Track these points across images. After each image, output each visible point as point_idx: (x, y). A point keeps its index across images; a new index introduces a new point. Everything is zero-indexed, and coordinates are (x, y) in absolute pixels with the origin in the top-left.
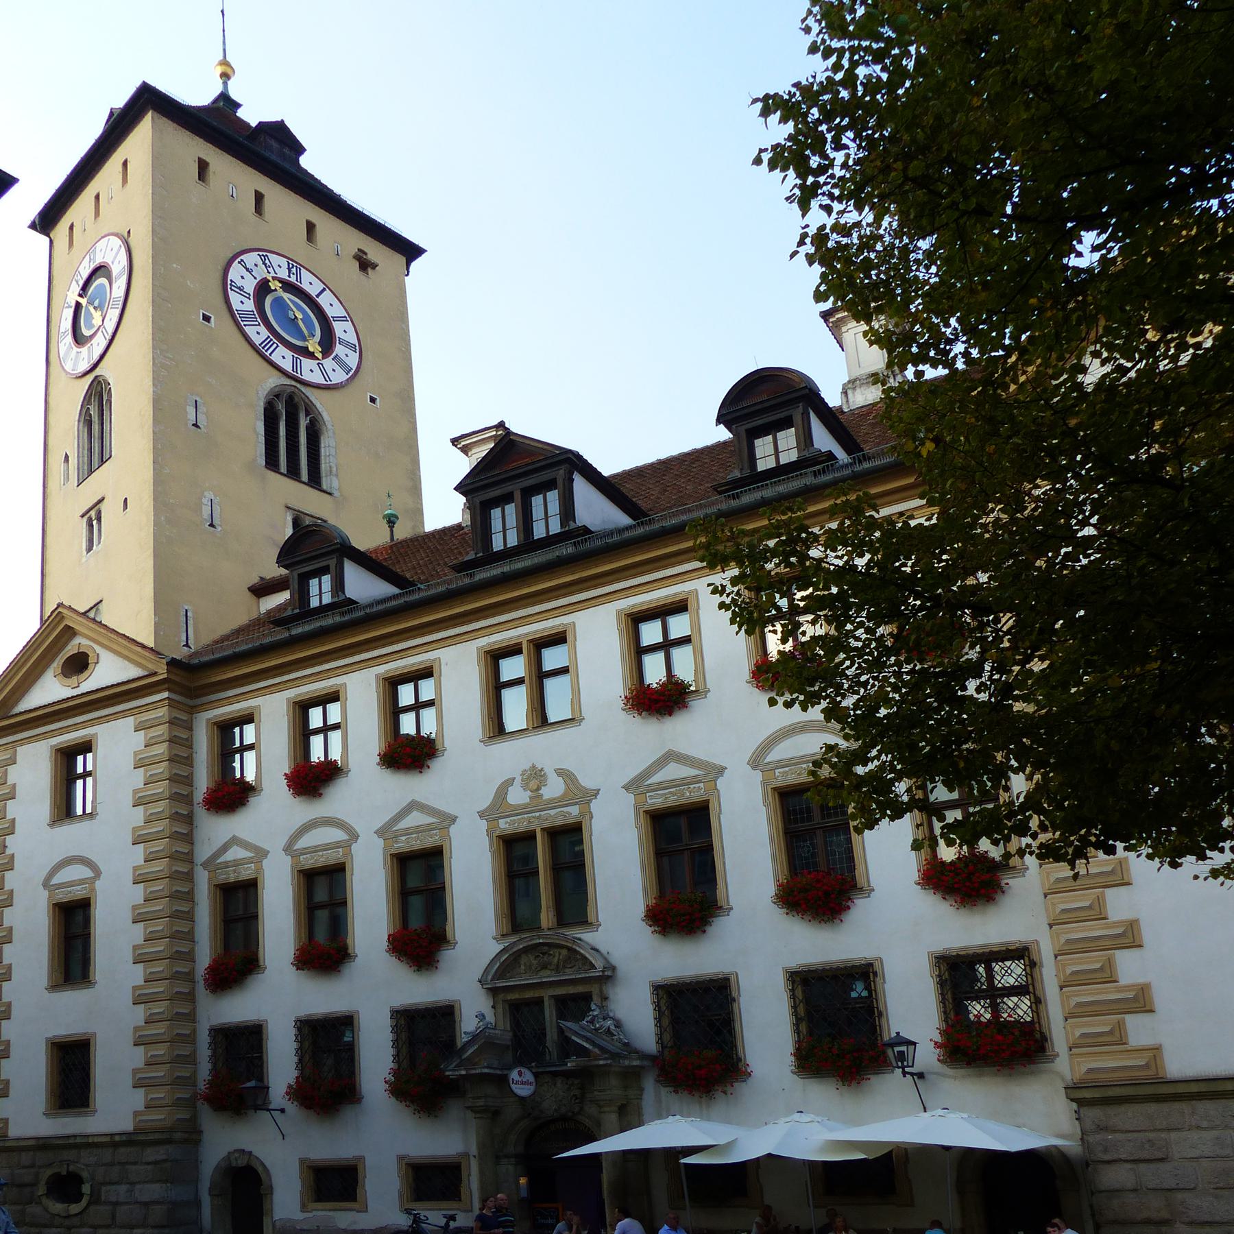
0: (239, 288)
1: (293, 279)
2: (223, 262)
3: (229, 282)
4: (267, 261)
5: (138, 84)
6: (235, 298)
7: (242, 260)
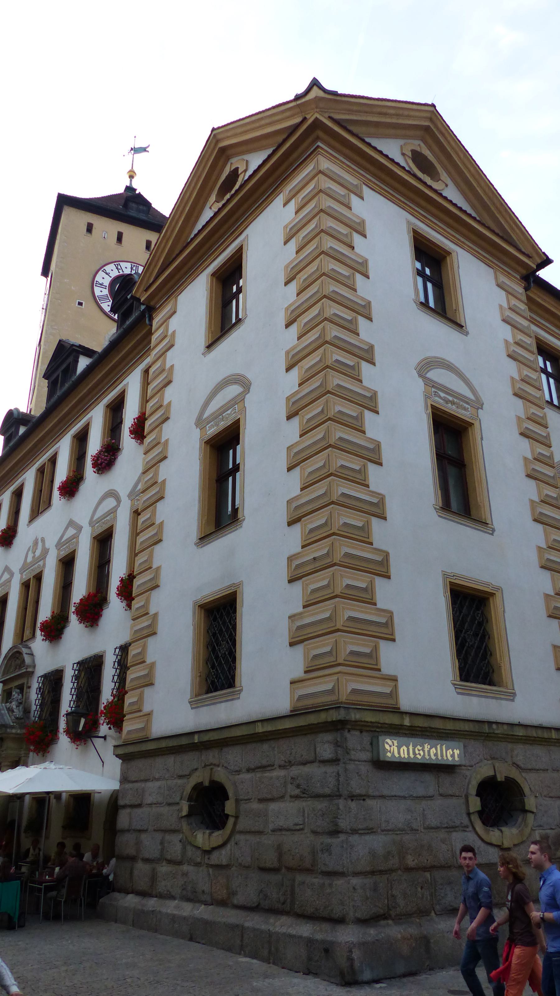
0: (101, 284)
2: (94, 273)
3: (95, 282)
4: (119, 267)
5: (57, 195)
6: (98, 291)
7: (104, 269)
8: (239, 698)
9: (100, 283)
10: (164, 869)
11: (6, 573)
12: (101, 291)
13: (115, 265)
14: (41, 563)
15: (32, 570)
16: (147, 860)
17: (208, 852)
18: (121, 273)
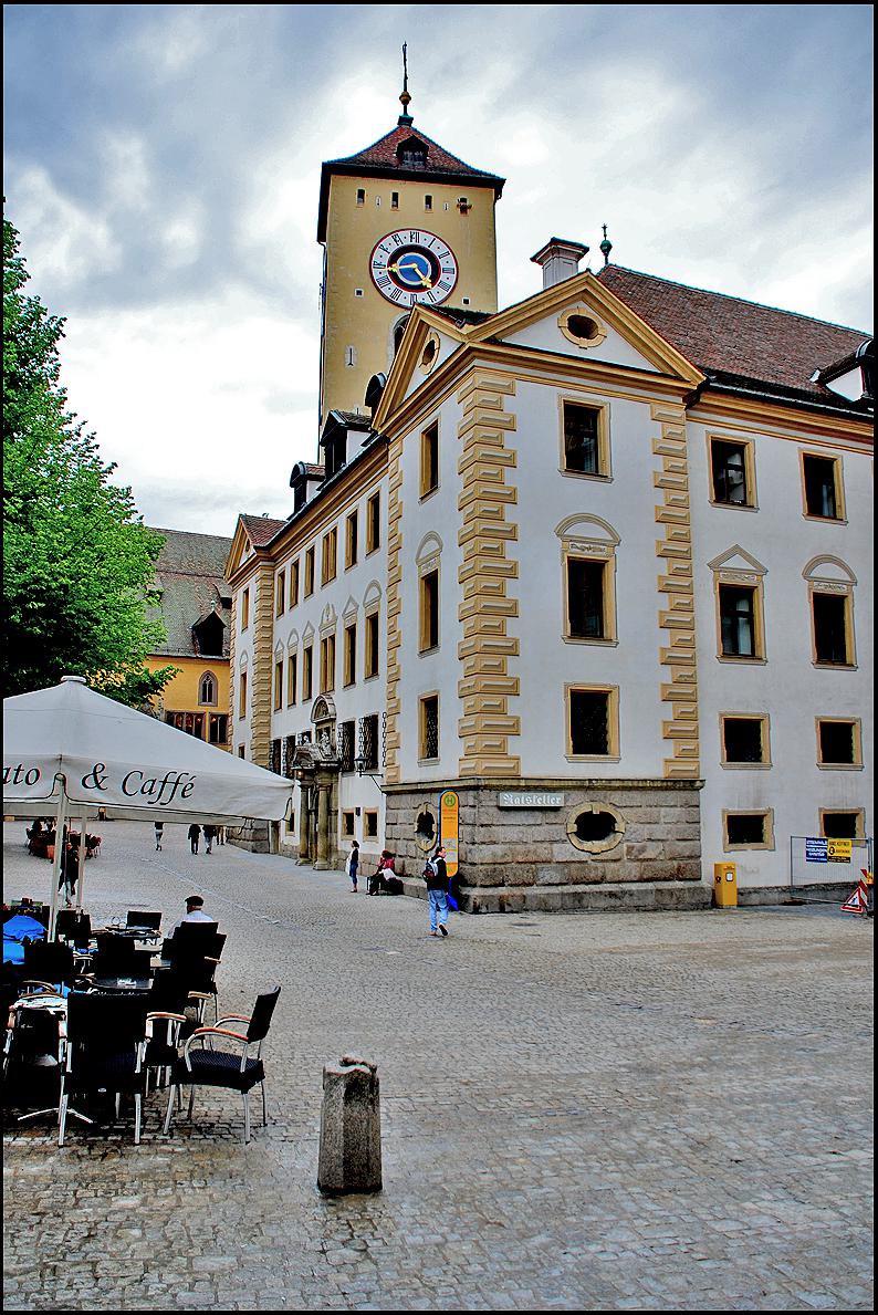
1: (414, 242)
10: (408, 861)
16: (400, 856)
17: (426, 852)
18: (400, 245)
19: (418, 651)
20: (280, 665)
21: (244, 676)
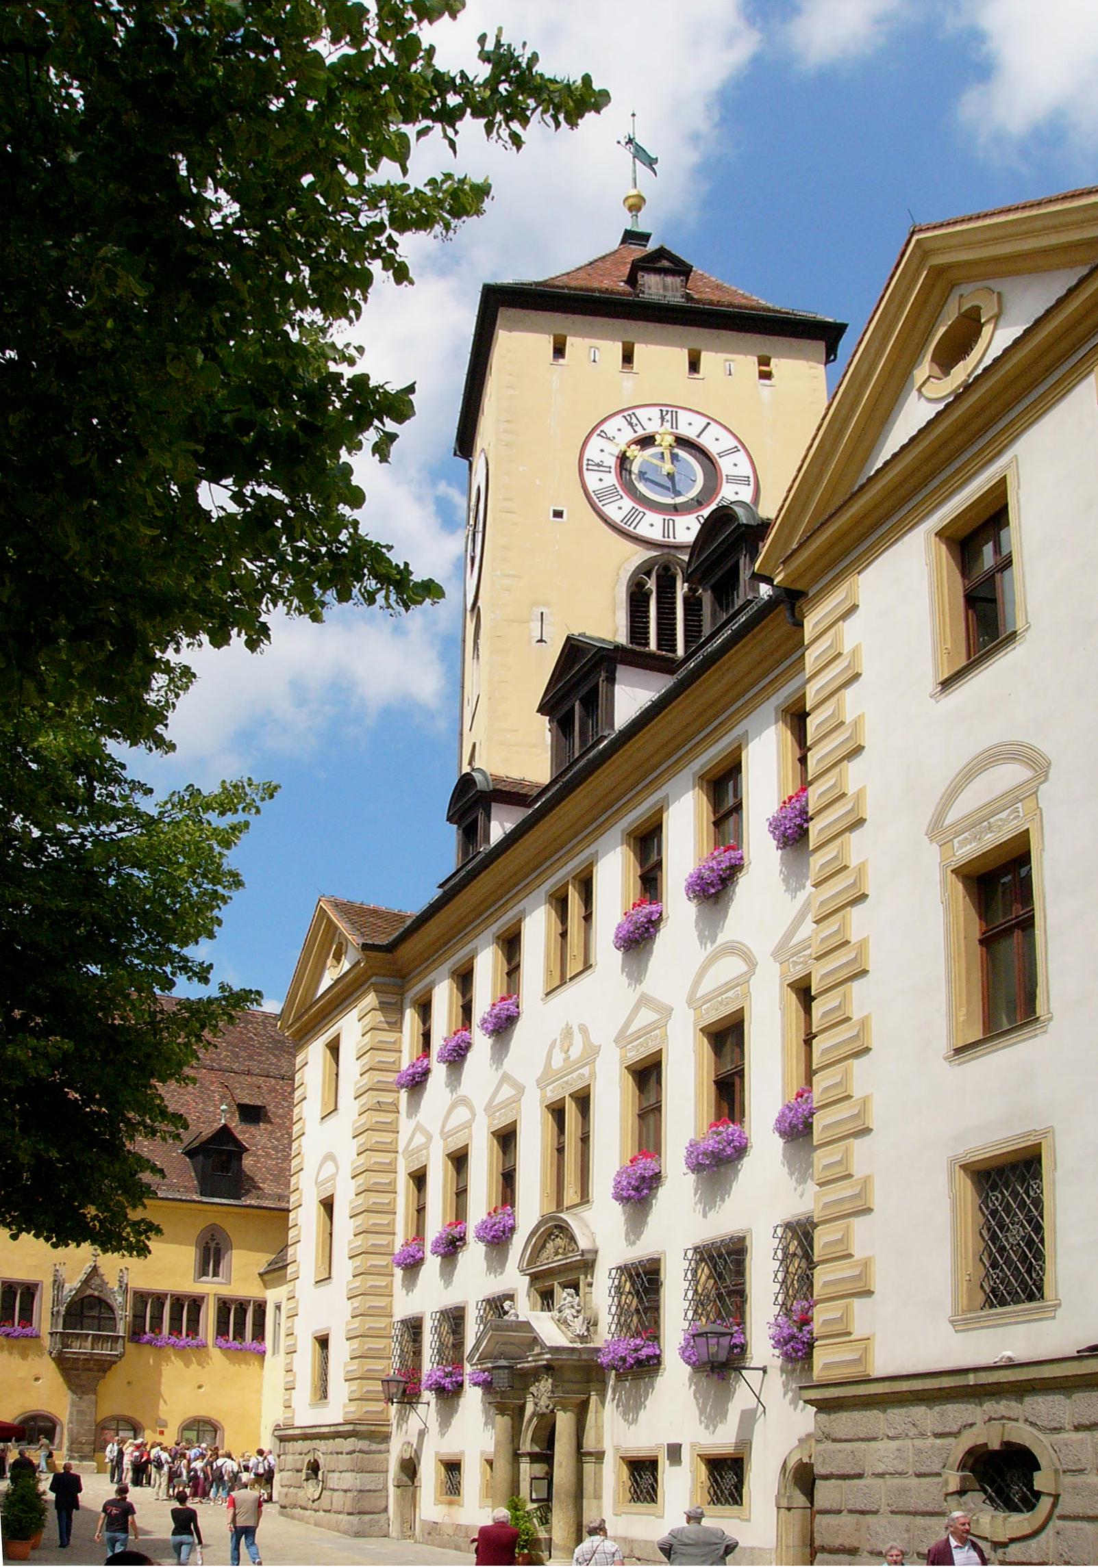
0: (598, 465)
4: (634, 421)
8: (1054, 1317)
9: (597, 461)
11: (505, 1086)
12: (601, 480)
13: (624, 417)
14: (585, 1071)
15: (566, 1083)
19: (943, 1046)
20: (419, 1179)
21: (328, 1205)
